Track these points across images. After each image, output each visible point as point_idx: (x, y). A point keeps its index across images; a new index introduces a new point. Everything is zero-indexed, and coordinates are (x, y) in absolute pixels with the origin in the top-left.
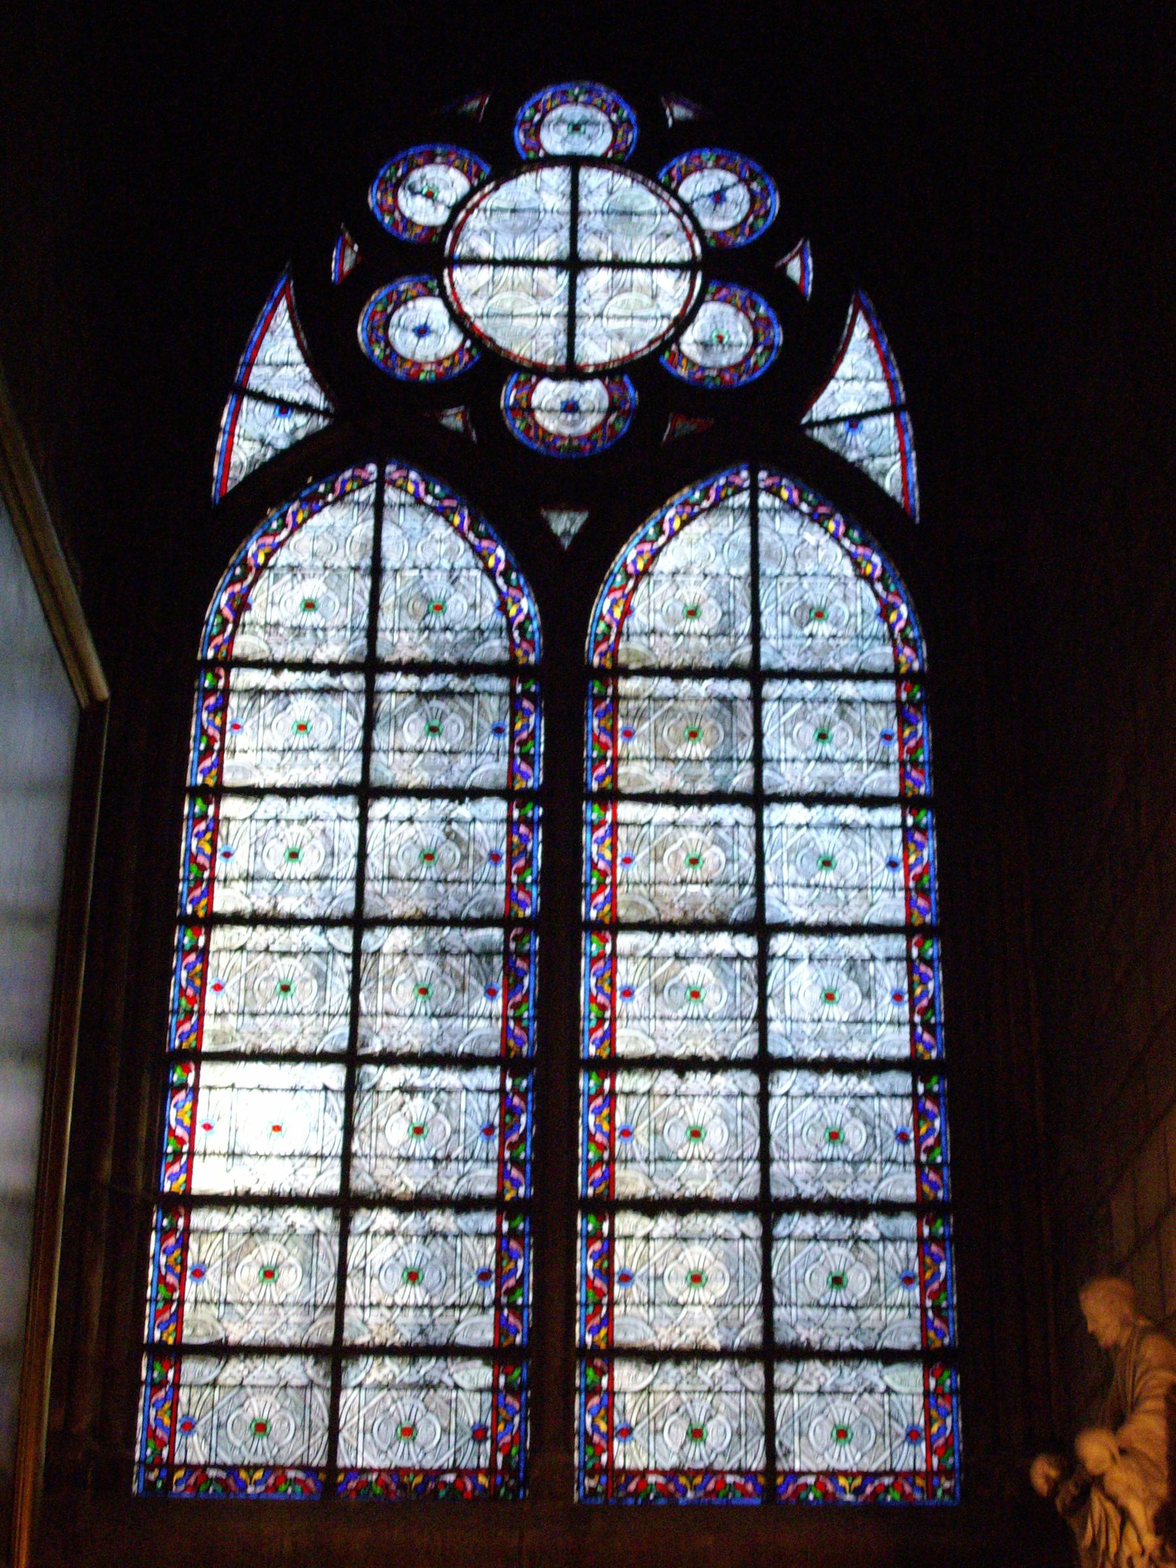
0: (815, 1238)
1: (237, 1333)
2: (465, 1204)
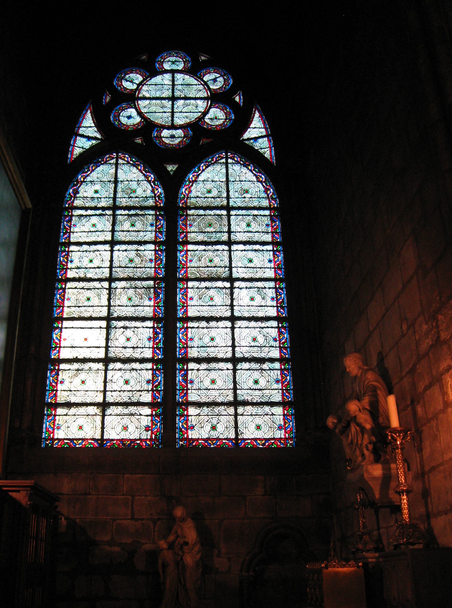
0: (249, 369)
1: (73, 400)
2: (143, 361)
